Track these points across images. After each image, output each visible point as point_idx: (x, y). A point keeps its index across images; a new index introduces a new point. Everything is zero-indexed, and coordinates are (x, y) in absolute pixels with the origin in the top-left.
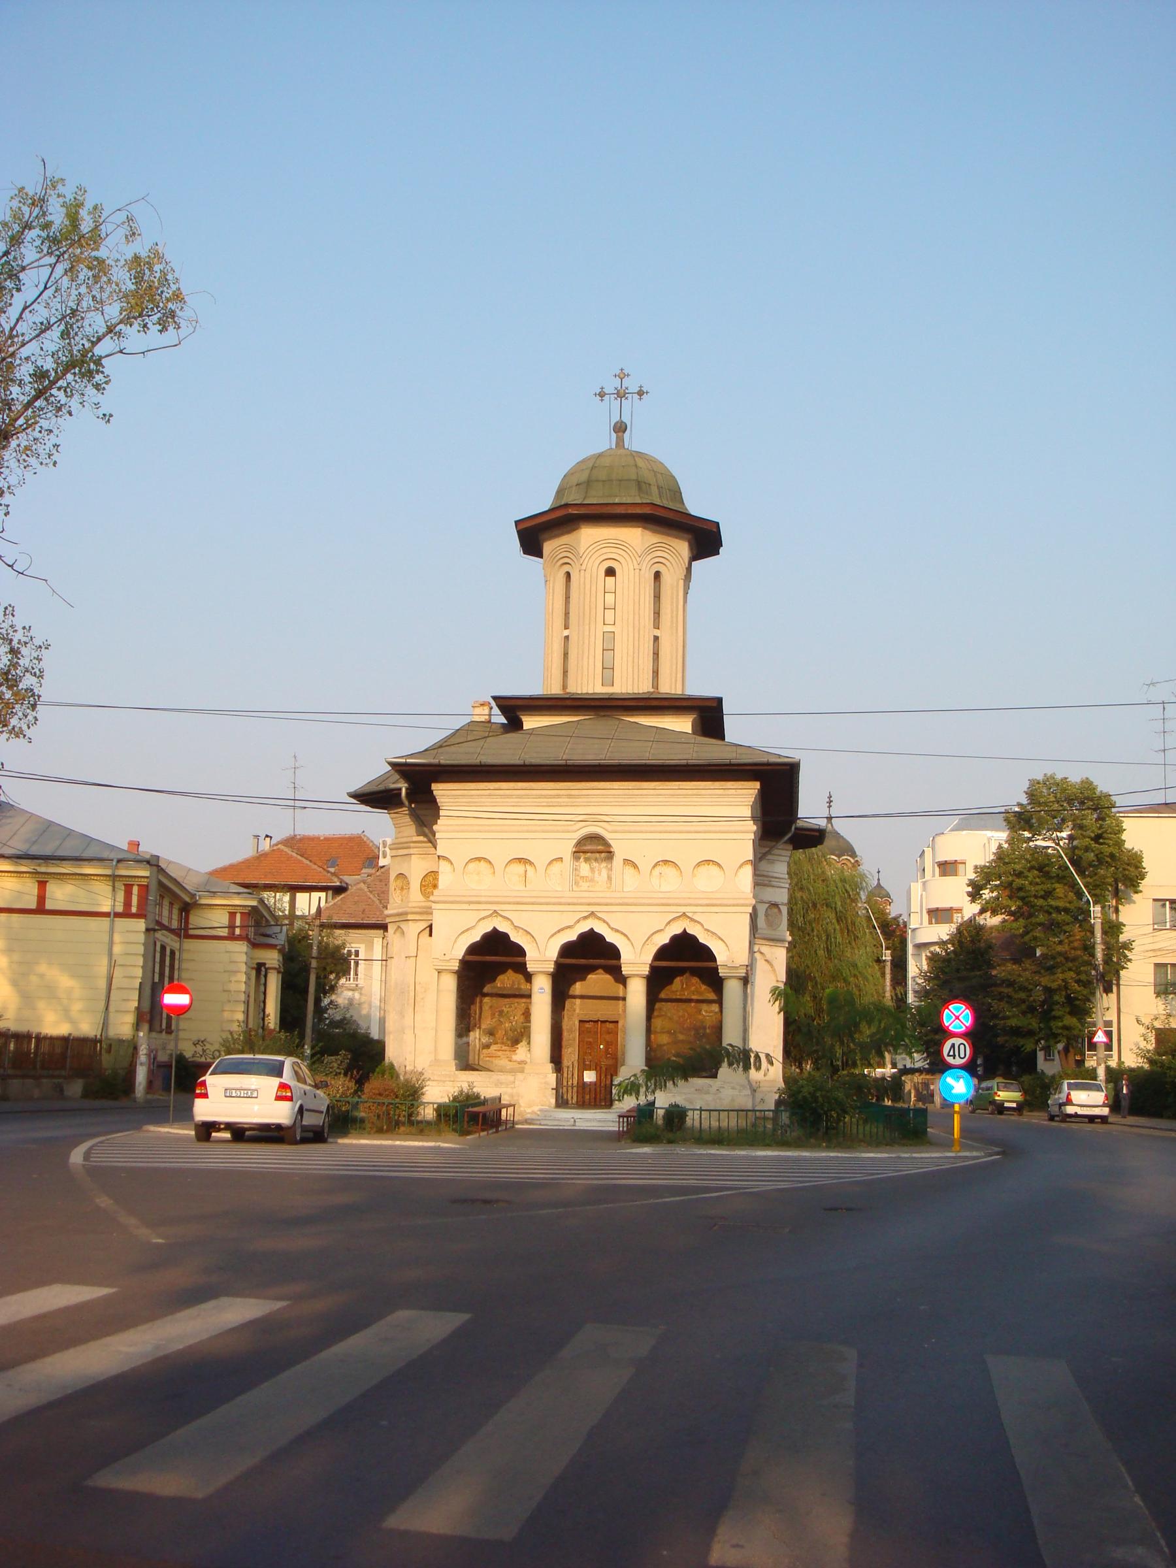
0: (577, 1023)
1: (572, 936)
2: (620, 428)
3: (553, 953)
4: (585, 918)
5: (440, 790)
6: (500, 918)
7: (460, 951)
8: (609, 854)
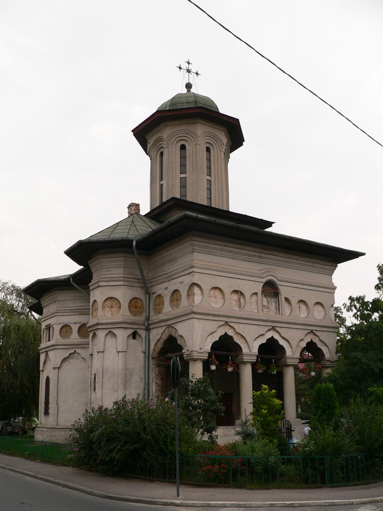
1: (263, 340)
2: (189, 86)
4: (269, 330)
6: (228, 327)
7: (208, 347)
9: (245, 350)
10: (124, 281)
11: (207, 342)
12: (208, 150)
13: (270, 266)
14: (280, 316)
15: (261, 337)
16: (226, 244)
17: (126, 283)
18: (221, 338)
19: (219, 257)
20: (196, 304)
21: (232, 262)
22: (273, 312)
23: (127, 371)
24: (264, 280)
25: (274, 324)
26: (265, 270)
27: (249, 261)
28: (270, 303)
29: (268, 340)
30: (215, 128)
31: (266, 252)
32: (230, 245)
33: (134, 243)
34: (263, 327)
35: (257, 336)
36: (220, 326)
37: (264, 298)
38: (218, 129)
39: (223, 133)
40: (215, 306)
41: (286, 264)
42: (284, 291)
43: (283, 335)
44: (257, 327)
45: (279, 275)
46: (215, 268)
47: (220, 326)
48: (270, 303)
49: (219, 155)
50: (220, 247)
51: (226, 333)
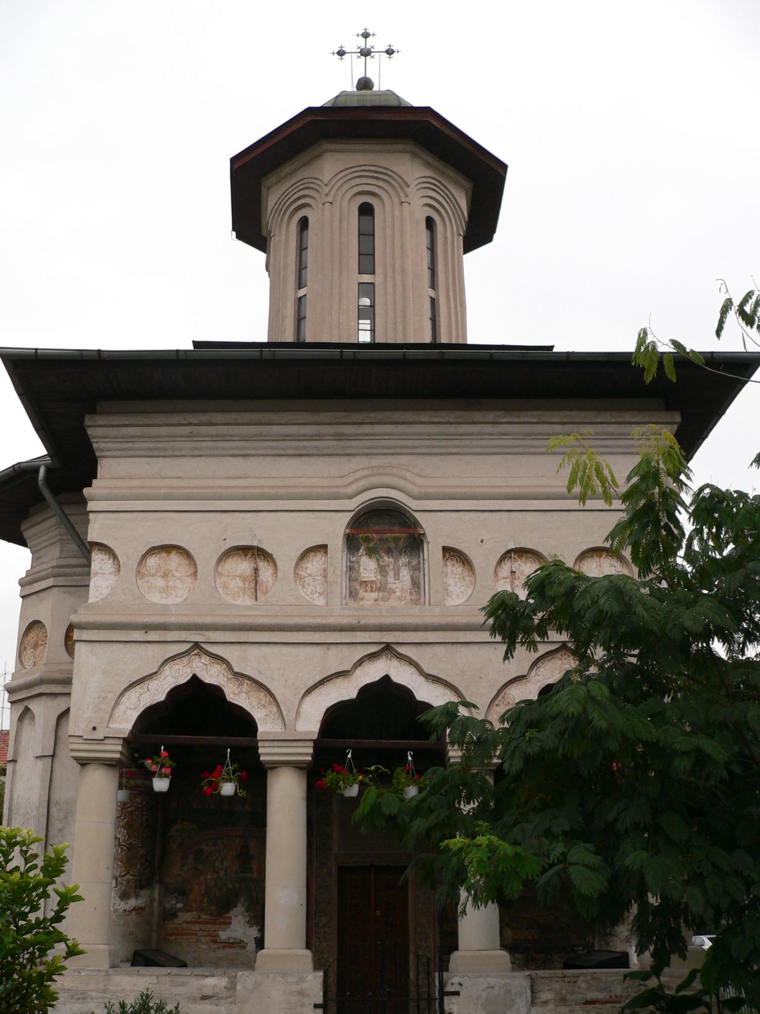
0: (334, 870)
1: (346, 691)
3: (310, 721)
4: (372, 656)
5: (101, 432)
6: (205, 659)
7: (125, 721)
8: (415, 542)
9: (267, 725)
10: (55, 576)
11: (121, 708)
12: (366, 210)
13: (388, 460)
14: (416, 610)
15: (339, 680)
16: (205, 417)
17: (60, 581)
18: (175, 693)
19: (190, 459)
20: (90, 601)
21: (237, 465)
22: (400, 599)
23: (54, 810)
24: (355, 504)
25: (388, 637)
26: (359, 474)
27: (301, 455)
28: (391, 574)
29: (365, 691)
30: (381, 151)
31: (357, 417)
32: (219, 417)
33: (42, 471)
34: (345, 649)
35: (318, 679)
36: (172, 658)
37: (365, 560)
38: (389, 151)
39: (407, 157)
40: (164, 602)
41: (449, 443)
42: (437, 530)
43: (427, 670)
44: (317, 650)
45: (420, 481)
46: (163, 491)
47: (172, 658)
48: (391, 574)
49: (397, 213)
50: (186, 430)
51: (194, 677)
